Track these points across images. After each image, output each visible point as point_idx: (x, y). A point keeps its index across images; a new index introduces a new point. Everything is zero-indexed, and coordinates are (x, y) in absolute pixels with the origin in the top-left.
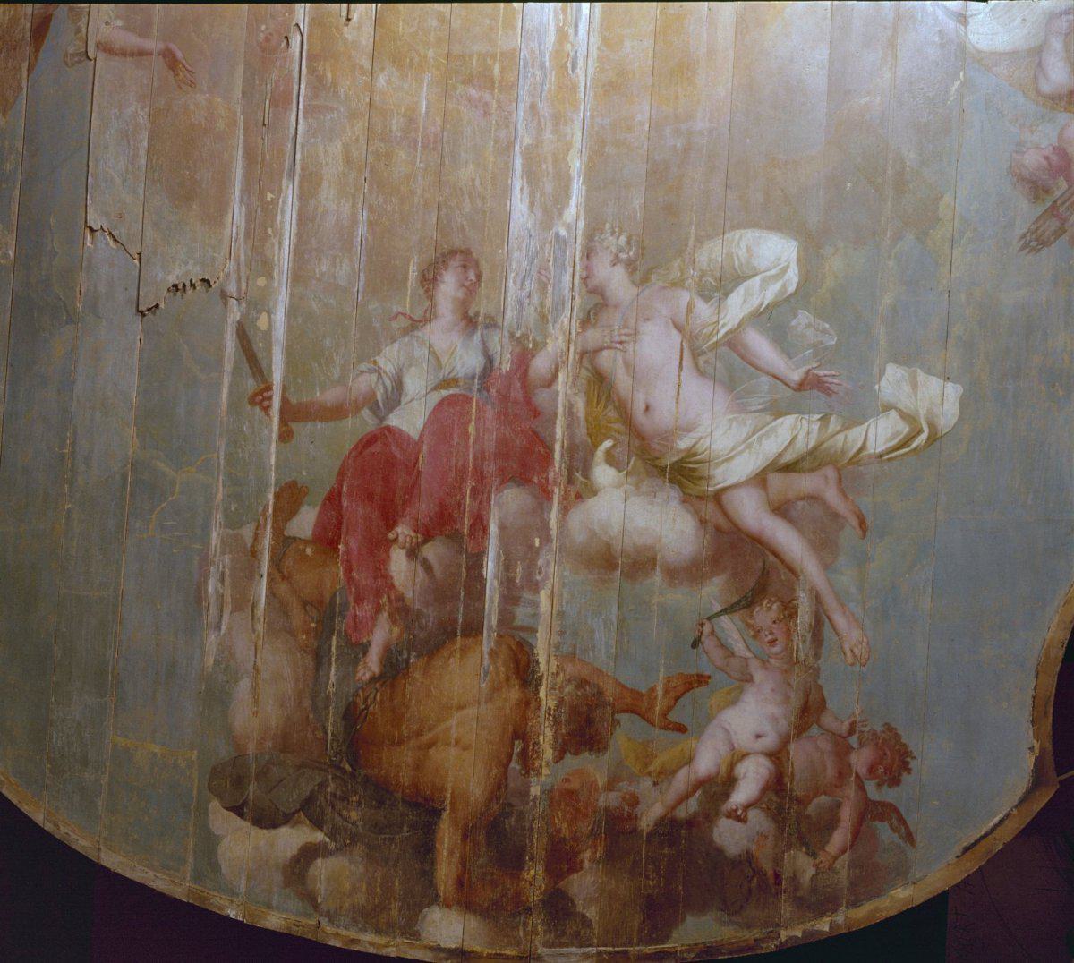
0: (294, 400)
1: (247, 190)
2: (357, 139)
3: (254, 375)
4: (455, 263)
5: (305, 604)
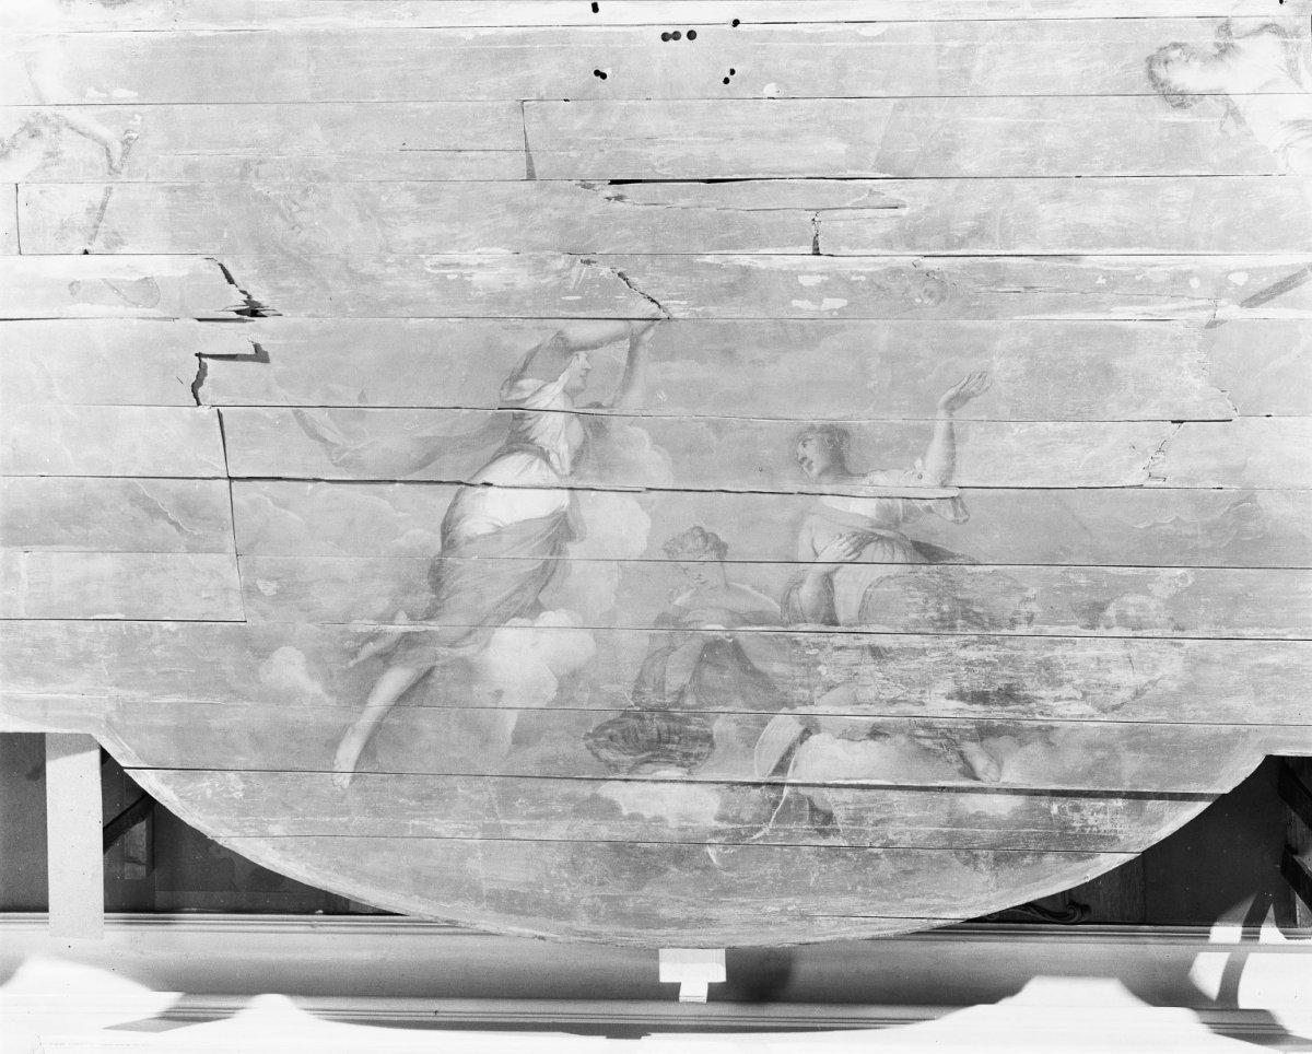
1: (1095, 306)
2: (1035, 188)
3: (1298, 285)
4: (1161, 72)
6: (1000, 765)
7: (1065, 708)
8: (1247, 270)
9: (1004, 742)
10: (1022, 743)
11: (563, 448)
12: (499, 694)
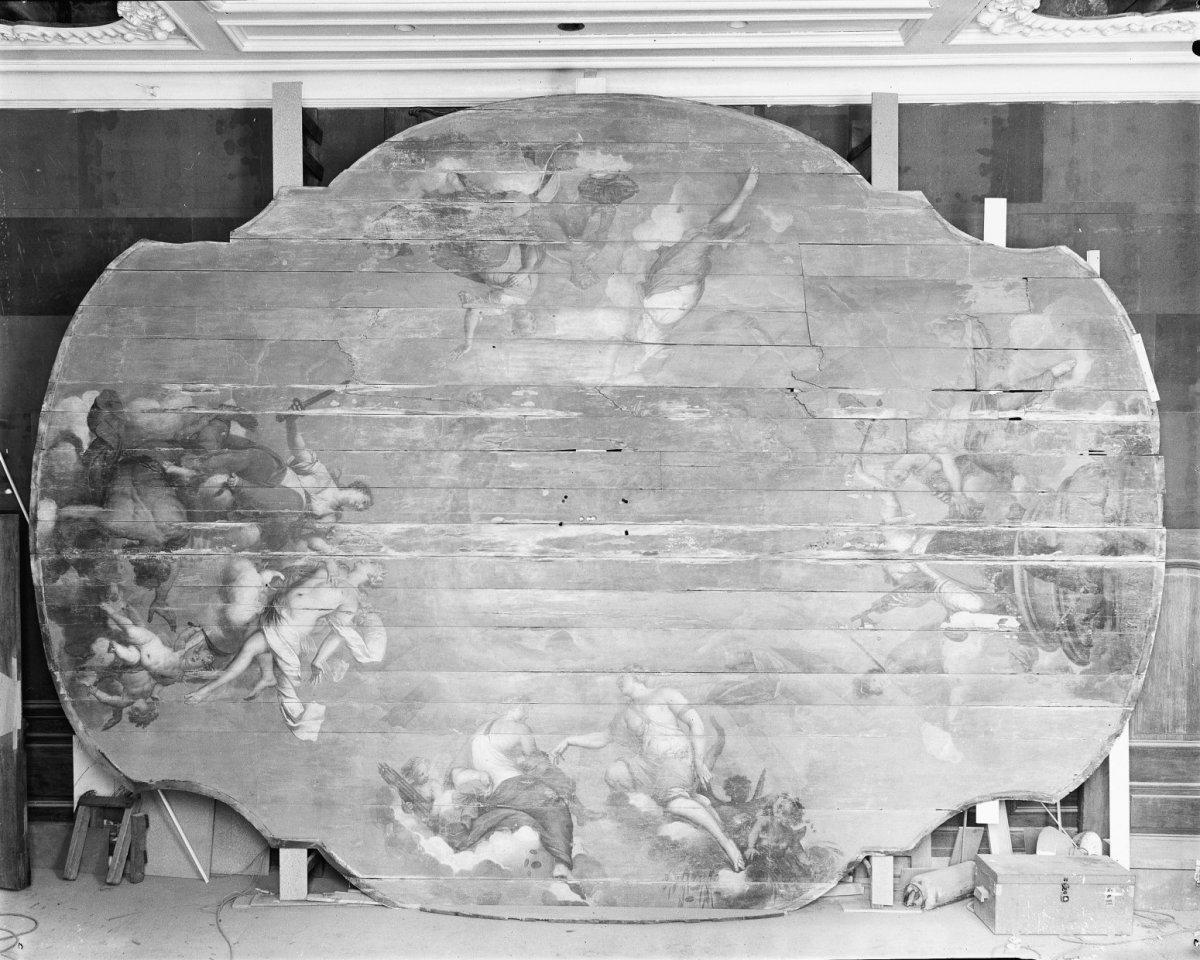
0: (297, 421)
1: (399, 390)
4: (367, 498)
5: (198, 433)
6: (447, 180)
7: (415, 206)
8: (331, 407)
9: (446, 191)
10: (437, 191)
11: (646, 326)
12: (678, 212)
